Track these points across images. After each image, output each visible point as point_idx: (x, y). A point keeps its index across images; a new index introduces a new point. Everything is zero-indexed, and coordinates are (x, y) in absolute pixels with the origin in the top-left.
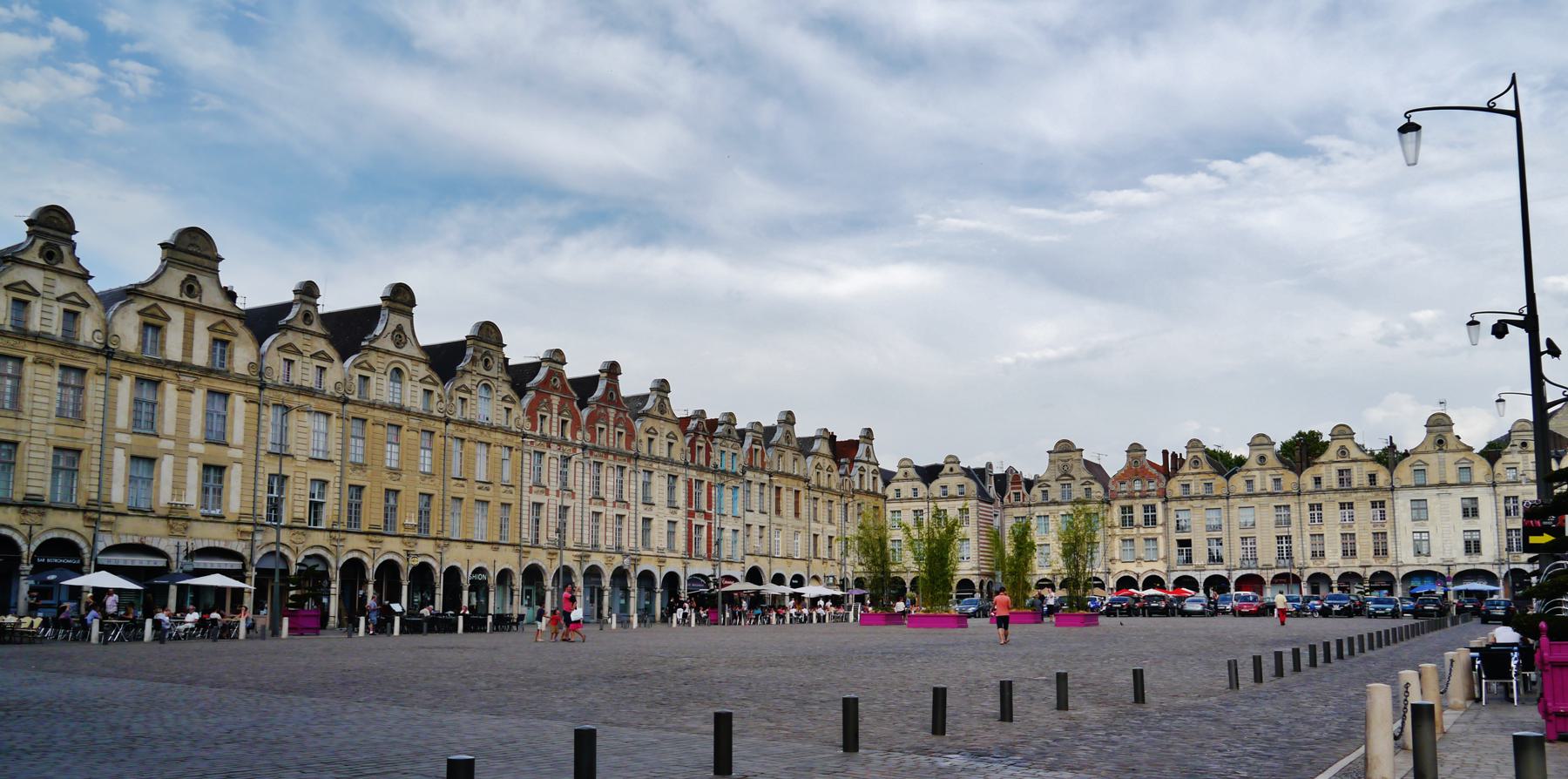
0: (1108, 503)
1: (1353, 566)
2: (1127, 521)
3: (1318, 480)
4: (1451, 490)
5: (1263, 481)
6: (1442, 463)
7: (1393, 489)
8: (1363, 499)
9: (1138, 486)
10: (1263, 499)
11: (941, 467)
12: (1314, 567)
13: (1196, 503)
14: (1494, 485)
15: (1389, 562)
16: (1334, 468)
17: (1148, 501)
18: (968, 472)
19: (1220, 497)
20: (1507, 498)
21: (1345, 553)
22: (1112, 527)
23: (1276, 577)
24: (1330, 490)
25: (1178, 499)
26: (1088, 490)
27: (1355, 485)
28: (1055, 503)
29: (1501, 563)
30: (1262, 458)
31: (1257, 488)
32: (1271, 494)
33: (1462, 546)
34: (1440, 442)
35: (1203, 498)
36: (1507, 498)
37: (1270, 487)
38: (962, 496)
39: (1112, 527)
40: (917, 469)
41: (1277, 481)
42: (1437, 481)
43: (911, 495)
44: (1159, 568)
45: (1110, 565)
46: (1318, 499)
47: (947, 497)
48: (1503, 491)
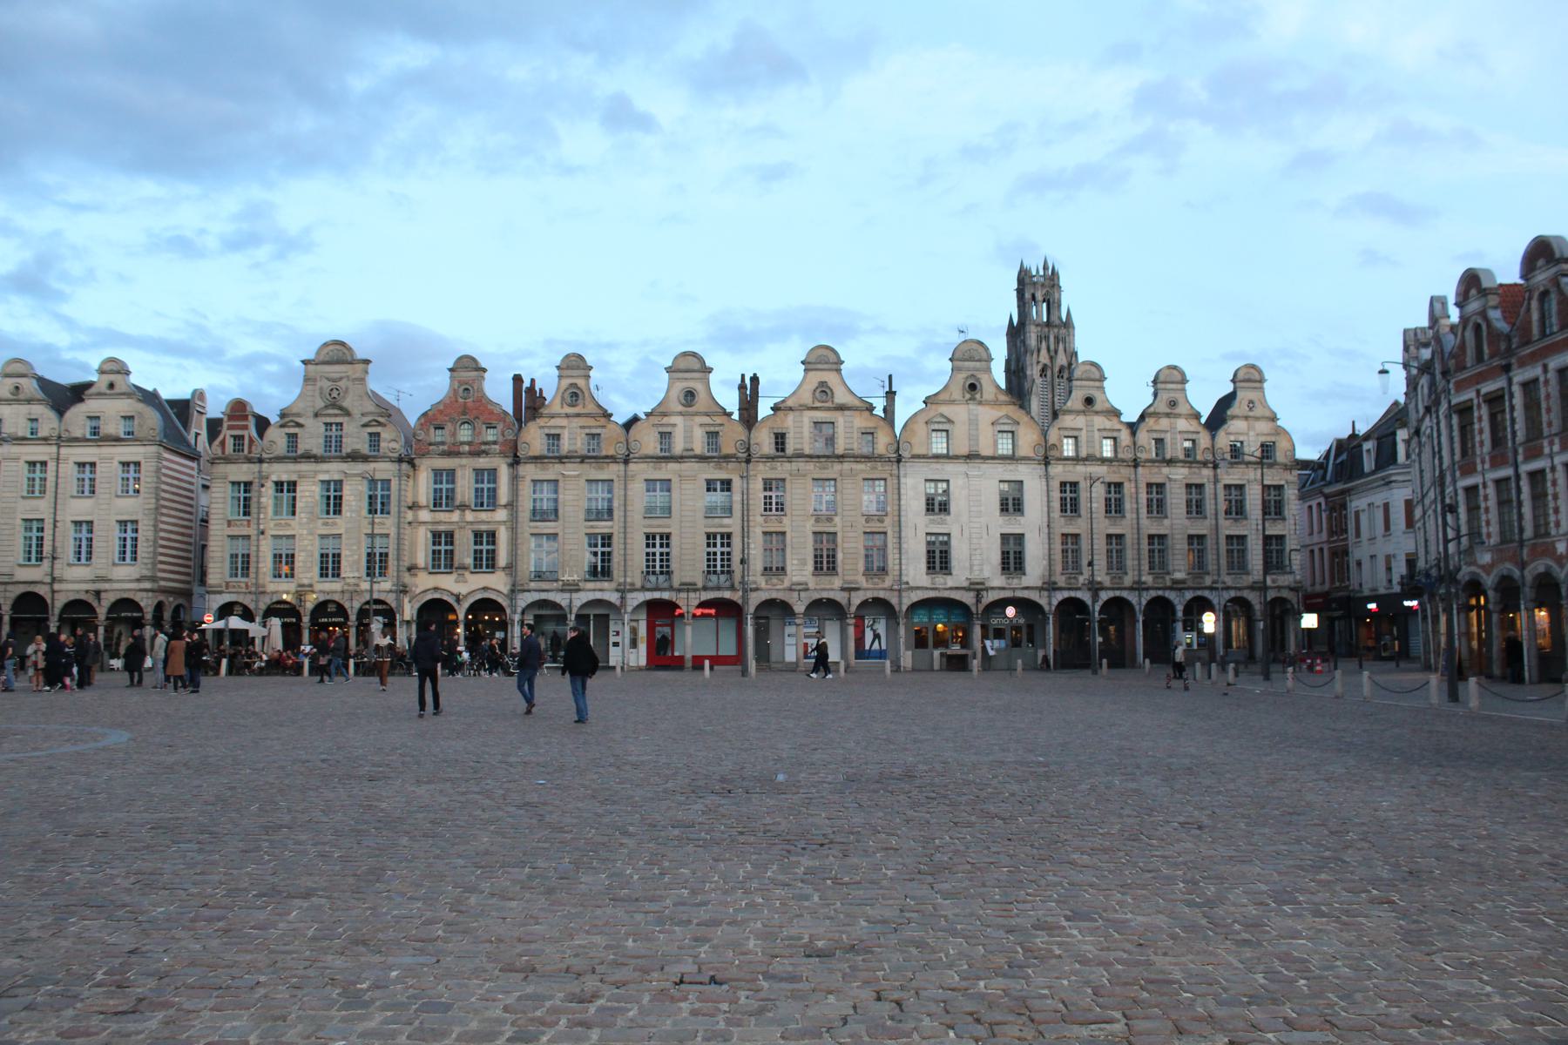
0: (411, 463)
1: (831, 587)
2: (443, 500)
3: (780, 440)
4: (987, 467)
5: (689, 437)
6: (973, 422)
7: (899, 461)
8: (852, 473)
9: (465, 434)
10: (689, 467)
11: (89, 385)
12: (766, 590)
13: (571, 470)
14: (1046, 462)
15: (888, 582)
16: (808, 417)
17: (483, 462)
18: (150, 398)
19: (612, 459)
20: (1063, 484)
21: (818, 568)
22: (414, 506)
23: (702, 605)
24: (800, 455)
25: (537, 459)
26: (375, 437)
27: (840, 450)
28: (308, 457)
29: (1050, 587)
30: (690, 395)
31: (678, 447)
32: (702, 458)
33: (996, 557)
34: (973, 387)
35: (583, 459)
36: (1063, 484)
37: (699, 447)
38: (130, 438)
39: (414, 506)
40: (44, 384)
41: (713, 435)
42: (964, 451)
43: (23, 430)
44: (496, 583)
45: (407, 578)
46: (782, 469)
47: (98, 437)
48: (1057, 470)
